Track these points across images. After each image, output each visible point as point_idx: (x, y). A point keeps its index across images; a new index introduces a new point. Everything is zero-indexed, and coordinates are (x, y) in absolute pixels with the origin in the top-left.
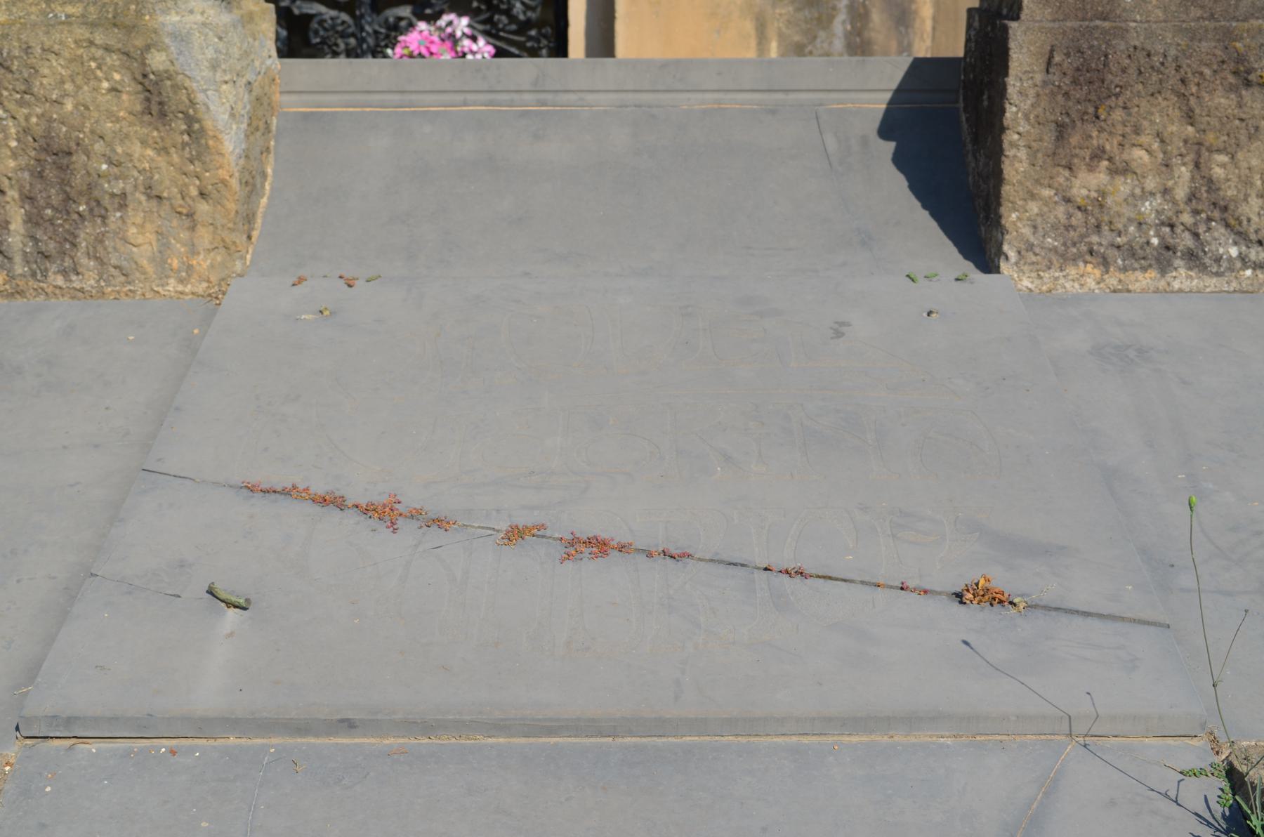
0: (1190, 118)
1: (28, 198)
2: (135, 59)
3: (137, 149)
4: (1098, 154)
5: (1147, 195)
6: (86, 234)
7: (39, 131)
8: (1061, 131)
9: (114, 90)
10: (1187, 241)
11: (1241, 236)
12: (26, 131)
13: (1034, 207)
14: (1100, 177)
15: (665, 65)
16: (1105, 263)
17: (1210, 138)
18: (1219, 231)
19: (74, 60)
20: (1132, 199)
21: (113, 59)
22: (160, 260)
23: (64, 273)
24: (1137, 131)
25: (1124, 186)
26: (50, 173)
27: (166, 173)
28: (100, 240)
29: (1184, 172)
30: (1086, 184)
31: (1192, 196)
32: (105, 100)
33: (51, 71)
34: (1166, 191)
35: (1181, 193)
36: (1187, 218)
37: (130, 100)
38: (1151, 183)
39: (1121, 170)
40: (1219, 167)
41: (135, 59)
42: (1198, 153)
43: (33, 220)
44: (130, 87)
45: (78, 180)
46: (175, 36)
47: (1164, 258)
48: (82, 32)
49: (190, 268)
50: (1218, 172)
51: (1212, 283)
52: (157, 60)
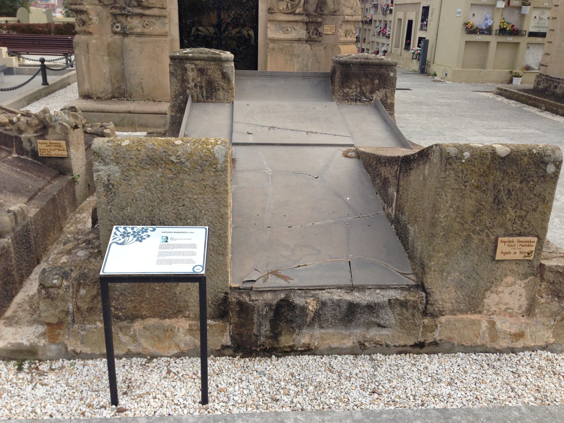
0: (359, 81)
1: (206, 89)
2: (221, 71)
3: (221, 82)
4: (348, 86)
5: (354, 92)
6: (214, 94)
7: (208, 80)
8: (343, 83)
9: (219, 74)
10: (359, 98)
11: (366, 98)
12: (206, 80)
13: (339, 93)
14: (348, 89)
15: (289, 72)
16: (348, 101)
17: (362, 84)
18: (363, 97)
19: (213, 70)
20: (352, 92)
21: (218, 70)
22: (224, 98)
23: (211, 99)
24: (353, 83)
25: (351, 91)
26: (209, 85)
27: (225, 86)
28: (216, 94)
29: (359, 89)
30: (346, 90)
31: (359, 92)
32: (217, 76)
33: (210, 72)
34: (356, 91)
35: (358, 92)
36: (359, 95)
37: (220, 76)
38: (354, 90)
39: (350, 88)
40: (363, 88)
41: (221, 71)
42: (361, 86)
43: (206, 92)
44: (220, 74)
45: (213, 86)
46: (227, 67)
47: (356, 101)
48: (215, 67)
49: (228, 99)
50: (363, 89)
51: (362, 104)
52: (224, 70)
